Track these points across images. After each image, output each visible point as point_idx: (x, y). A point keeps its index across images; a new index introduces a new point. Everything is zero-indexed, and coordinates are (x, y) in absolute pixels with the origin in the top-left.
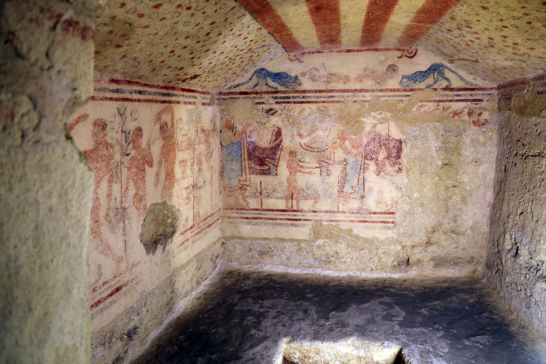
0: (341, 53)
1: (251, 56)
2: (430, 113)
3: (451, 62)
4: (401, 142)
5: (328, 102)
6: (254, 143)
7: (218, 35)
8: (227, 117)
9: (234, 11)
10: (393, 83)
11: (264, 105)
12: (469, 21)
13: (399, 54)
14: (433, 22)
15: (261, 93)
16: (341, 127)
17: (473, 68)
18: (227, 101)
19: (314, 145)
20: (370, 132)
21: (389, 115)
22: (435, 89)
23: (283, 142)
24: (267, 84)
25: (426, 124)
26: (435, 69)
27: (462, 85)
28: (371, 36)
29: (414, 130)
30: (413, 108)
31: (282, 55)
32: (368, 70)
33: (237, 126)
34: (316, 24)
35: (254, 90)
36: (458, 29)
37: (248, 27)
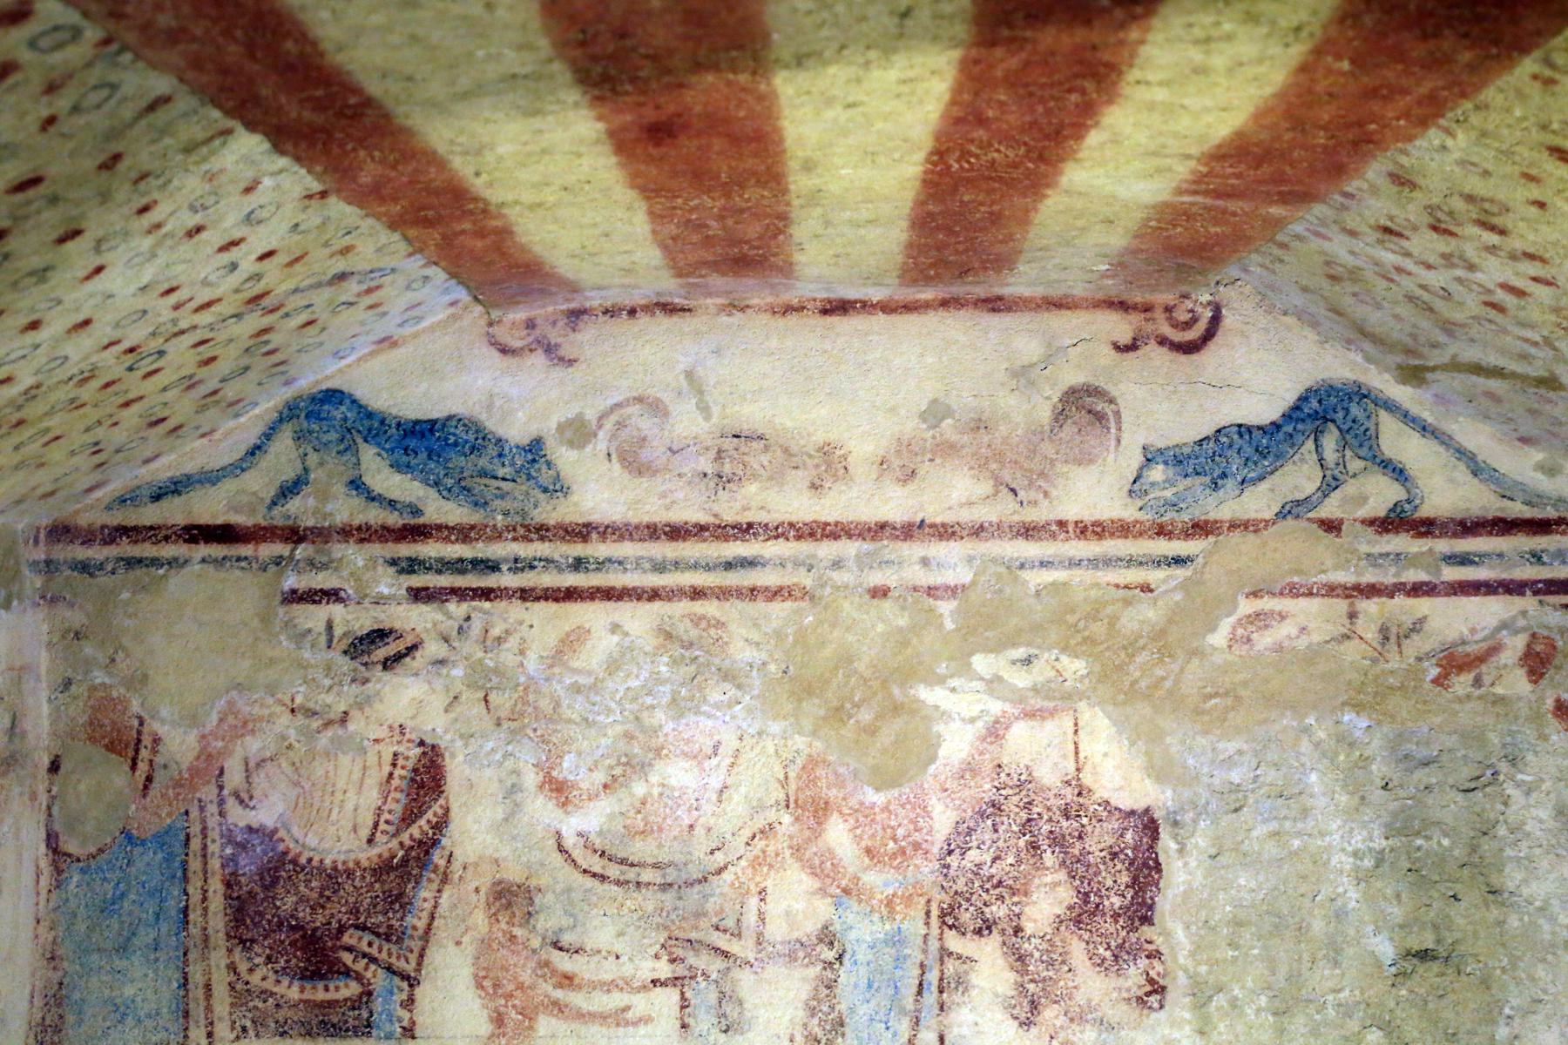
0: (793, 319)
1: (266, 331)
2: (1311, 656)
3: (1414, 375)
4: (1150, 826)
5: (724, 594)
6: (269, 835)
7: (62, 240)
8: (99, 677)
9: (161, 116)
10: (1094, 489)
11: (337, 610)
12: (1492, 201)
13: (1121, 327)
14: (1302, 197)
15: (320, 535)
16: (800, 742)
17: (1532, 412)
18: (103, 580)
19: (640, 849)
20: (969, 770)
21: (1075, 667)
22: (1331, 526)
23: (454, 828)
24: (356, 485)
25: (1288, 721)
26: (1322, 412)
27: (1476, 499)
28: (961, 236)
29: (1219, 756)
30: (1213, 629)
31: (454, 318)
32: (949, 412)
33: (162, 730)
34: (649, 191)
35: (278, 517)
36: (1435, 228)
37: (248, 190)
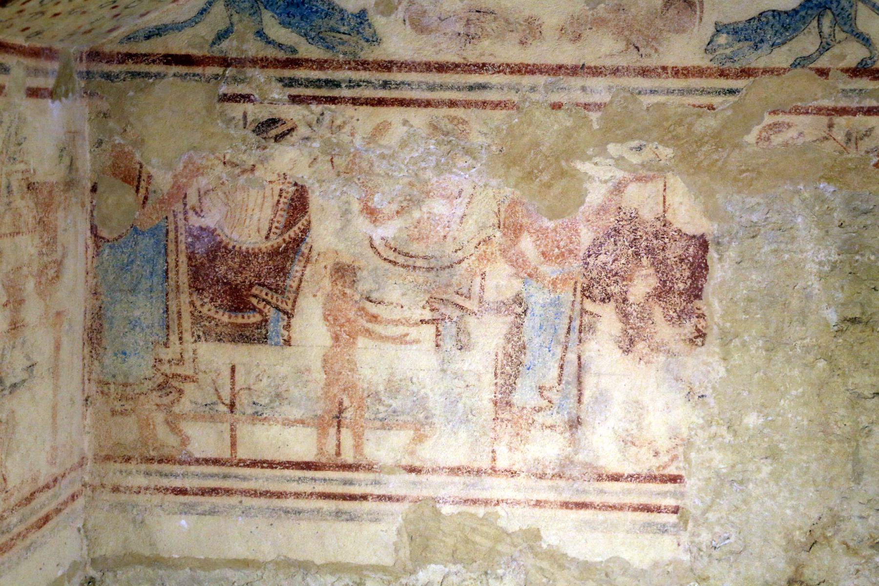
2: (803, 150)
4: (703, 244)
5: (467, 104)
8: (118, 140)
11: (249, 107)
15: (240, 63)
16: (508, 191)
19: (416, 248)
20: (602, 210)
21: (667, 152)
22: (823, 73)
24: (260, 34)
25: (788, 187)
29: (745, 206)
30: (748, 131)
33: (153, 171)
35: (216, 51)
